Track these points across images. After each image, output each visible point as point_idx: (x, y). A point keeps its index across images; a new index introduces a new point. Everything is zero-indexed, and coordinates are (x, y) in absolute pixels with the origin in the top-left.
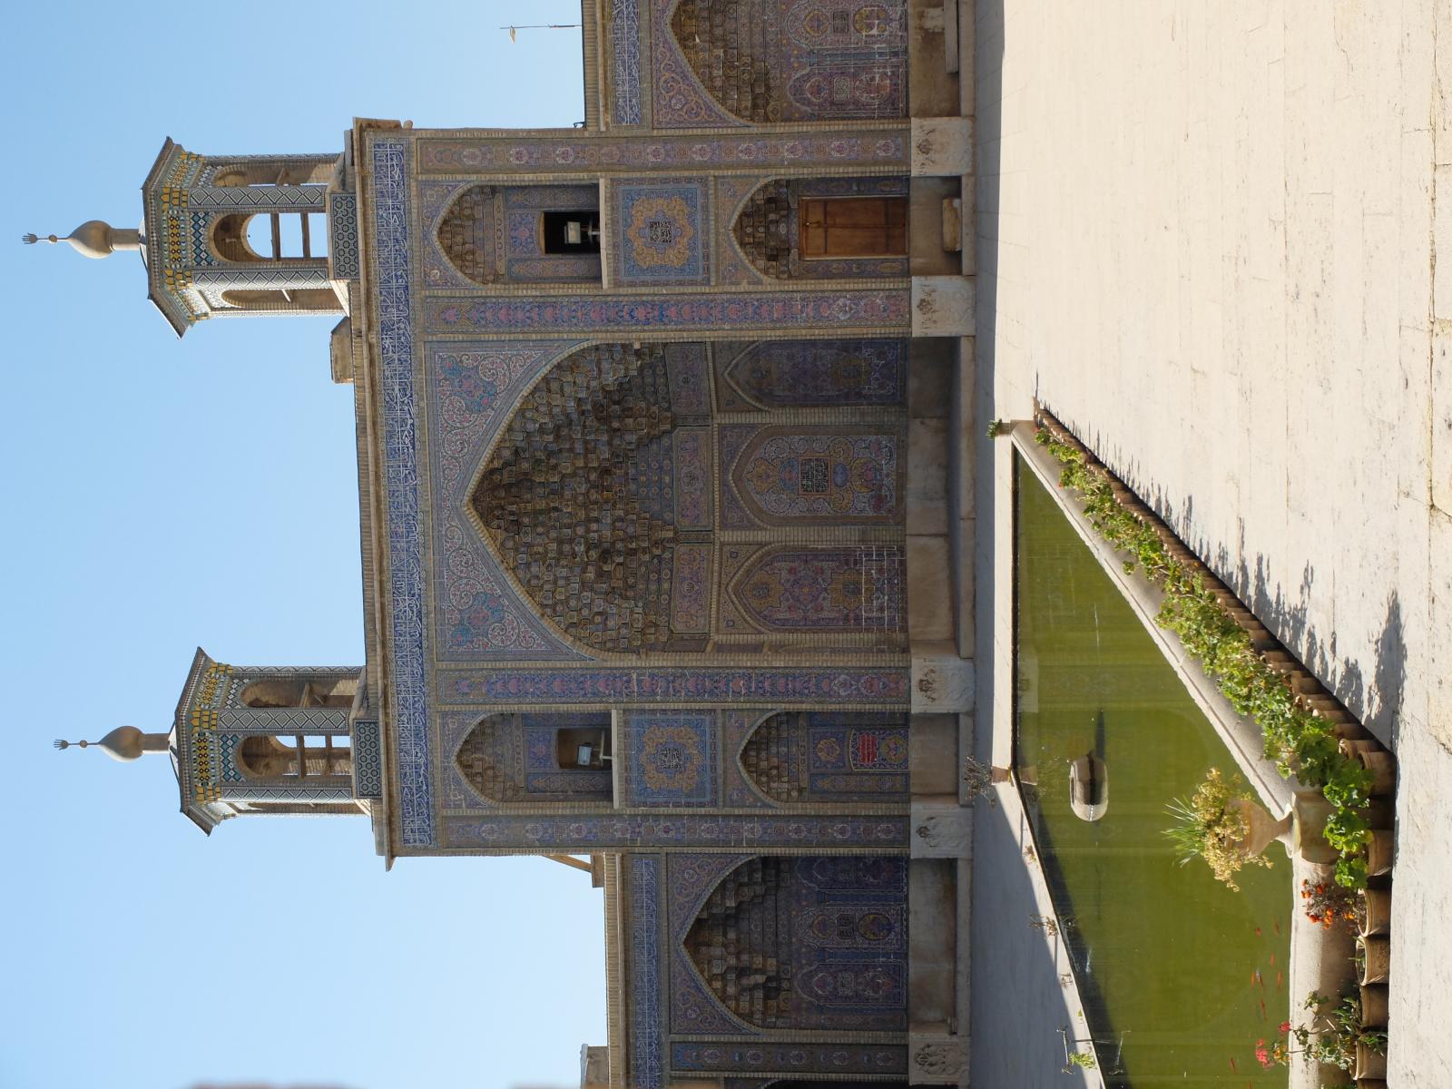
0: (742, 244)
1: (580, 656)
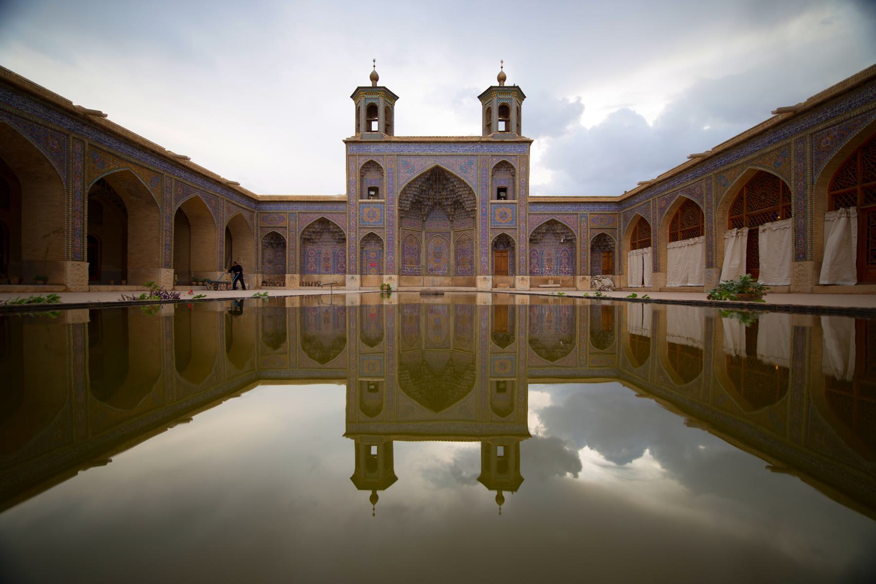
0: (499, 236)
1: (398, 191)
